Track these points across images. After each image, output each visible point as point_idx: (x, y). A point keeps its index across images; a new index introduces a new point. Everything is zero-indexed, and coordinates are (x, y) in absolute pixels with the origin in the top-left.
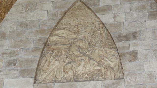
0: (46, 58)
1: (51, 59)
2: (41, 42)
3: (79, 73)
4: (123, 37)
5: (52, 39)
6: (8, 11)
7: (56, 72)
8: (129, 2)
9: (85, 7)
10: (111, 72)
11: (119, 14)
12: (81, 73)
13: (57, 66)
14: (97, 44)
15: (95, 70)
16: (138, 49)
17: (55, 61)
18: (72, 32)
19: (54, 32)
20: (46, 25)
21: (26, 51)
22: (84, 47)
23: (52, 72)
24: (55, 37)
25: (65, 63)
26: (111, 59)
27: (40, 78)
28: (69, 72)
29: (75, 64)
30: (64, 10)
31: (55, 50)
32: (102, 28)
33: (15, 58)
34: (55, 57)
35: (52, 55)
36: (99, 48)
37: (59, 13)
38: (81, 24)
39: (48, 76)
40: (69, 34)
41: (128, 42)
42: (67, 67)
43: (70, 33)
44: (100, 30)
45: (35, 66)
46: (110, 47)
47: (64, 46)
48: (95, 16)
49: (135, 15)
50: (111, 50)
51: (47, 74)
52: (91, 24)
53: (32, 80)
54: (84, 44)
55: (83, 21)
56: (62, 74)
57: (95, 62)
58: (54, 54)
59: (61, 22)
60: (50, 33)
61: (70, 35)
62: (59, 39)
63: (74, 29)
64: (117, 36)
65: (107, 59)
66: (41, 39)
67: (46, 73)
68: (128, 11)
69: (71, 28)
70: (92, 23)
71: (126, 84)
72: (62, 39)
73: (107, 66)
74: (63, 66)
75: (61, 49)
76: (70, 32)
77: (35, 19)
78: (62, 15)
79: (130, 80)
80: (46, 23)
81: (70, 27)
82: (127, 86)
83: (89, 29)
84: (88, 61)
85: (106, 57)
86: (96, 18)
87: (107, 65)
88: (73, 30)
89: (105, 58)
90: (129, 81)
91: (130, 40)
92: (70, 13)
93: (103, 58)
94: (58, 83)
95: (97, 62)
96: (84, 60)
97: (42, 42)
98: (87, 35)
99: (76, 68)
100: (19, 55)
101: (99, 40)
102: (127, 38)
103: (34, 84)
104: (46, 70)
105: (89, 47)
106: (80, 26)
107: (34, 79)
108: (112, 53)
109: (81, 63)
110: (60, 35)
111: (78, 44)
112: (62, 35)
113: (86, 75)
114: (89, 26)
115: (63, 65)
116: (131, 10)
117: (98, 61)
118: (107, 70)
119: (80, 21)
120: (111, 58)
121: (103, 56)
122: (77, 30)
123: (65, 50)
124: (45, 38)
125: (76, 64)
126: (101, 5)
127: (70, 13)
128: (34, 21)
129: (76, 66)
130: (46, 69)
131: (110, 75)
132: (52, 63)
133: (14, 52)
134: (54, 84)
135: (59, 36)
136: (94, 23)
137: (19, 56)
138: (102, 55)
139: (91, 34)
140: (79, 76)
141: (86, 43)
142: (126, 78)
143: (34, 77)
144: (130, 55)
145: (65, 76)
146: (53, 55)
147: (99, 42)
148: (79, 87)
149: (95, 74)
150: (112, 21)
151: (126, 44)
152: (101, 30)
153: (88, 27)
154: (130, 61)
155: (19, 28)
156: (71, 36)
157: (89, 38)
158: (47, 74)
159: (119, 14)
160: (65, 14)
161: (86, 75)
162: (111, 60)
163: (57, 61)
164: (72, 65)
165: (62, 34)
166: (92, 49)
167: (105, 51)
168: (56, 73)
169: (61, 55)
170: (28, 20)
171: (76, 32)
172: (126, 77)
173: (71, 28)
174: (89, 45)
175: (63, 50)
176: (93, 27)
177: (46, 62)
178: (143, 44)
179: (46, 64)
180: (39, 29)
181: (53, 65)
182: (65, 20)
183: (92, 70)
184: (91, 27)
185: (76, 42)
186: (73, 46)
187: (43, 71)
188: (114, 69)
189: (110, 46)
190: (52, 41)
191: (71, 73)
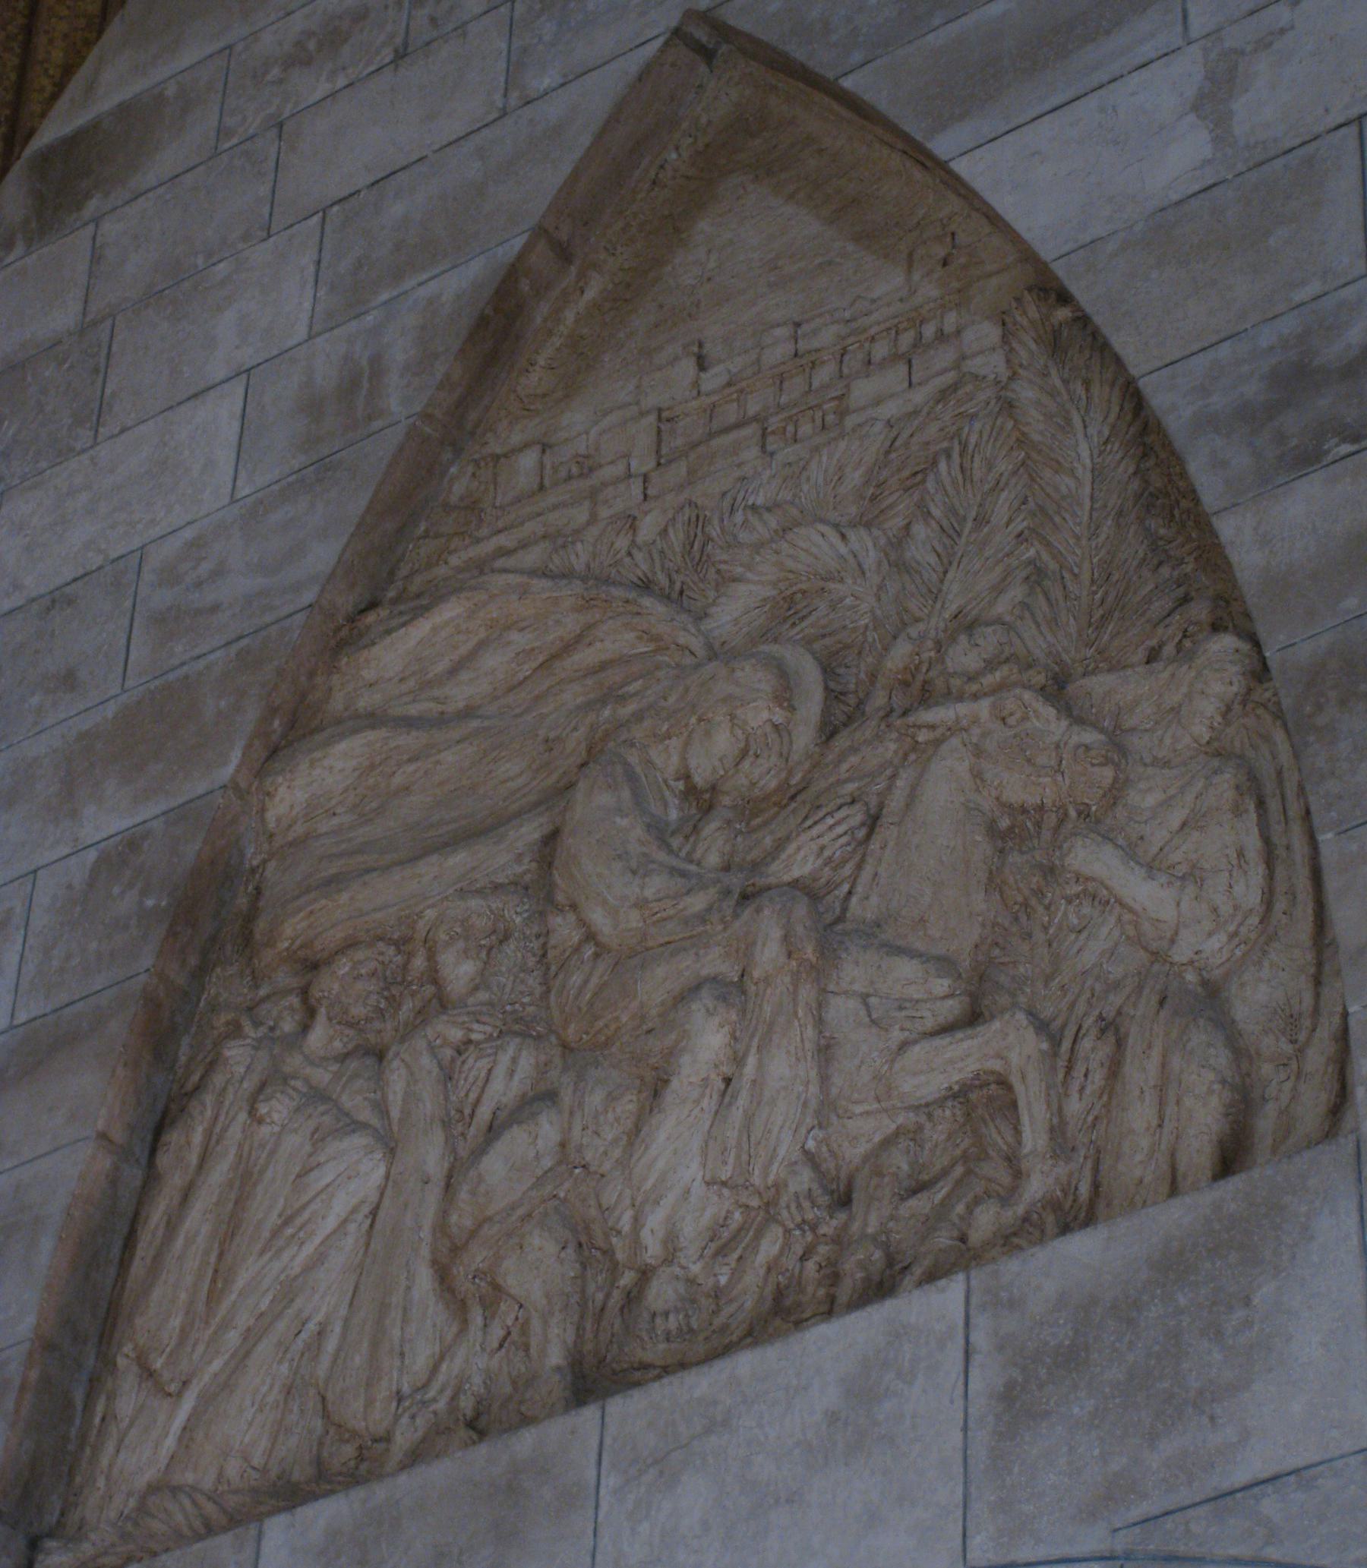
0: (197, 1138)
3: (653, 1248)
5: (301, 796)
12: (691, 1230)
15: (927, 1108)
17: (319, 1138)
19: (336, 679)
24: (343, 746)
28: (515, 1277)
34: (337, 1076)
36: (984, 707)
37: (400, 351)
47: (458, 860)
54: (760, 715)
59: (459, 483)
61: (568, 647)
62: (398, 780)
63: (632, 523)
64: (1252, 390)
66: (133, 842)
67: (185, 1383)
69: (594, 531)
80: (219, 572)
81: (581, 515)
87: (1116, 971)
88: (622, 543)
92: (590, 294)
95: (945, 964)
99: (607, 1166)
110: (413, 710)
111: (667, 759)
112: (460, 693)
114: (863, 390)
118: (1105, 1050)
123: (481, 923)
125: (611, 1098)
127: (590, 294)
128: (58, 600)
130: (176, 1322)
135: (409, 723)
138: (1041, 808)
148: (610, 1481)
156: (585, 657)
171: (661, 578)
177: (187, 1195)
180: (111, 710)
181: (287, 1223)
184: (890, 409)
188: (1241, 1012)
190: (299, 829)
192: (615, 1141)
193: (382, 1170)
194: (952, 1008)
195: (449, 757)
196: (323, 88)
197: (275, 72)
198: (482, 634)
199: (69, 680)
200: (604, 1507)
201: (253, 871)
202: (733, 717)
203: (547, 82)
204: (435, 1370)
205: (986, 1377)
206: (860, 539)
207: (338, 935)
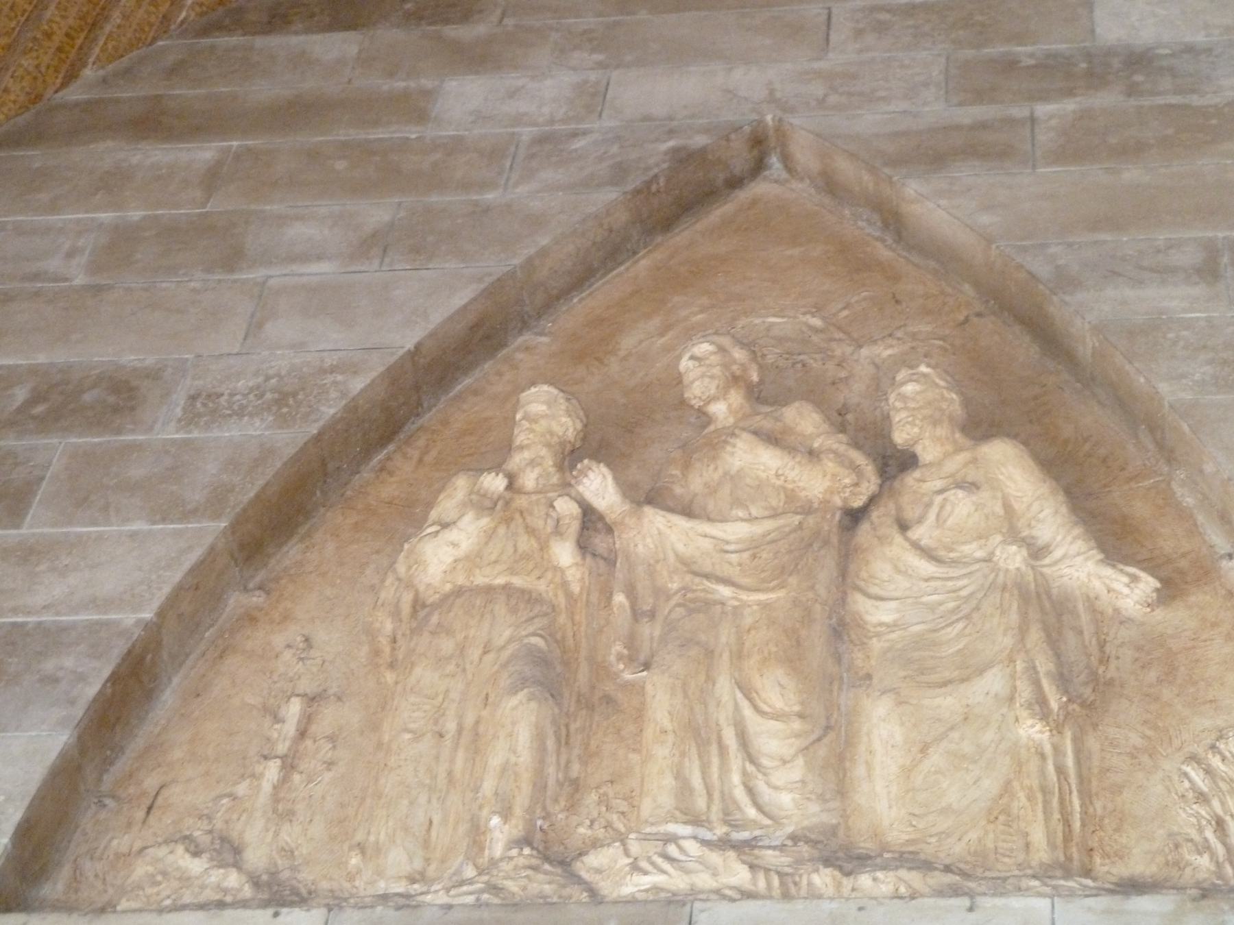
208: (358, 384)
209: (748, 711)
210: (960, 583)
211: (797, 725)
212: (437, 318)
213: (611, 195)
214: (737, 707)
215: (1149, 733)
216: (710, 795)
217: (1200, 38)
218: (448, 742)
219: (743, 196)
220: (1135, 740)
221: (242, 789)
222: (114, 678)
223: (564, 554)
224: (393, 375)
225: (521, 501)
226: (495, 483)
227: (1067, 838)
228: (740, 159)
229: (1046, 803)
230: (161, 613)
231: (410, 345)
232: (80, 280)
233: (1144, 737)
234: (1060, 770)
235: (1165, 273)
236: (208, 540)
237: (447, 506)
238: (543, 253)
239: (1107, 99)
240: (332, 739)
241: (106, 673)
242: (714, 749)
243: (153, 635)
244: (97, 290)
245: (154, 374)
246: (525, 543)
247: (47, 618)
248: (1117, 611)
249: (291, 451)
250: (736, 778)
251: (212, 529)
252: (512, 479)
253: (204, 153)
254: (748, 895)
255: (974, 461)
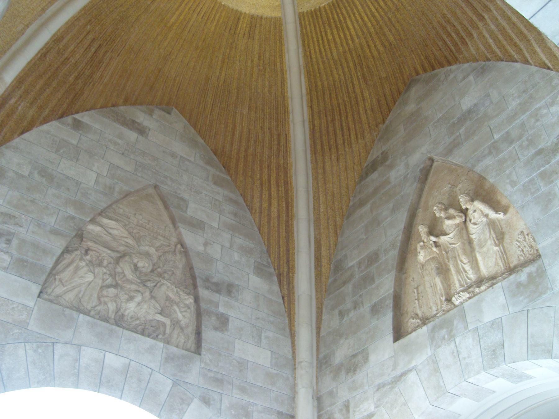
1: (81, 264)
2: (72, 225)
4: (212, 283)
6: (22, 133)
7: (82, 293)
8: (231, 232)
9: (159, 203)
10: (181, 334)
11: (214, 242)
13: (88, 281)
14: (166, 275)
16: (231, 313)
18: (130, 233)
20: (89, 199)
21: (39, 226)
22: (144, 270)
23: (76, 290)
25: (104, 284)
26: (185, 311)
27: (49, 291)
28: (110, 305)
29: (123, 293)
30: (126, 188)
31: (93, 250)
32: (180, 252)
33: (12, 228)
35: (84, 258)
37: (117, 189)
38: (147, 228)
39: (67, 294)
40: (123, 235)
41: (218, 295)
42: (107, 292)
43: (126, 234)
44: (176, 254)
45: (49, 263)
46: (186, 290)
47: (109, 252)
48: (171, 226)
49: (236, 256)
50: (187, 297)
51: (67, 289)
52: (162, 236)
53: (36, 289)
55: (151, 224)
56: (94, 302)
57: (157, 306)
58: (88, 257)
60: (92, 216)
61: (124, 237)
65: (177, 309)
67: (66, 286)
68: (227, 245)
69: (129, 226)
70: (165, 235)
71: (203, 366)
72: (108, 238)
73: (174, 321)
74: (99, 287)
75: (103, 255)
76: (127, 233)
77: (70, 176)
78: (122, 196)
79: (210, 361)
82: (203, 368)
83: (158, 244)
84: (147, 299)
85: (177, 304)
86: (172, 230)
87: (175, 319)
89: (175, 307)
90: (208, 361)
91: (221, 293)
93: (171, 305)
94: (87, 316)
96: (142, 294)
97: (75, 225)
98: (152, 250)
99: (123, 301)
100: (21, 226)
101: (170, 270)
102: (217, 287)
103: (38, 299)
104: (67, 281)
105: (152, 274)
106: (145, 230)
107: (40, 287)
108: (187, 302)
109: (136, 297)
112: (111, 231)
113: (138, 322)
114: (159, 237)
115: (100, 285)
116: (231, 246)
117: (162, 305)
119: (146, 221)
120: (184, 310)
121: (171, 300)
122: (137, 235)
123: (109, 260)
124: (81, 220)
125: (126, 294)
126: (188, 213)
128: (68, 178)
129: (123, 297)
131: (177, 338)
132: (81, 273)
133: (14, 216)
134: (79, 315)
135: (106, 231)
136: (168, 238)
137: (21, 229)
139: (160, 254)
140: (125, 318)
141: (149, 265)
142: (204, 355)
143: (42, 284)
144: (218, 318)
145: (99, 308)
146: (86, 259)
147: (170, 273)
148: (123, 338)
149: (152, 327)
150: (201, 248)
151: (216, 297)
152: (178, 255)
153: (156, 238)
154: (216, 329)
155: (36, 176)
156: (125, 240)
157: (155, 258)
158: (65, 288)
159: (212, 243)
160: (127, 195)
161: (138, 322)
162: (184, 313)
163: (92, 274)
164: (117, 294)
165: (111, 228)
166: (156, 280)
167: (177, 294)
168: (83, 296)
169: (100, 265)
170: (58, 170)
172: (204, 353)
173: (128, 225)
174: (152, 271)
175: (106, 258)
176: (165, 243)
178: (239, 309)
179: (69, 270)
180: (73, 199)
181: (82, 277)
182: (121, 206)
183: (150, 317)
184: (162, 242)
185: (134, 256)
186: (127, 258)
187: (61, 280)
189: (186, 288)
190: (90, 231)
191: (112, 306)
192: (124, 299)
193: (93, 279)
194: (159, 311)
195: (108, 237)
196: (112, 148)
197: (107, 140)
198: (116, 227)
199: (68, 189)
200: (122, 340)
201: (83, 230)
202: (144, 263)
203: (139, 175)
204: (96, 306)
205: (164, 355)
206: (157, 253)
207: (95, 249)
208: (400, 238)
209: (463, 264)
210: (480, 227)
211: (469, 264)
212: (404, 220)
213: (415, 184)
214: (461, 264)
215: (510, 239)
216: (463, 280)
217: (476, 101)
218: (433, 287)
219: (433, 167)
220: (509, 241)
221: (415, 306)
222: (394, 301)
223: (434, 249)
224: (404, 233)
225: (426, 244)
226: (422, 244)
227: (505, 263)
228: (429, 163)
229: (501, 259)
230: (394, 288)
231: (403, 227)
232: (365, 237)
233: (510, 240)
234: (502, 252)
235: (484, 157)
236: (394, 275)
237: (419, 249)
238: (412, 200)
239: (468, 123)
240: (421, 293)
241: (392, 301)
242: (461, 273)
243: (395, 291)
244: (367, 238)
245: (378, 250)
246: (430, 250)
247: (383, 296)
248: (501, 219)
249: (397, 254)
250: (465, 276)
251: (394, 273)
252: (424, 242)
253: (368, 206)
254: (470, 298)
255: (474, 206)
